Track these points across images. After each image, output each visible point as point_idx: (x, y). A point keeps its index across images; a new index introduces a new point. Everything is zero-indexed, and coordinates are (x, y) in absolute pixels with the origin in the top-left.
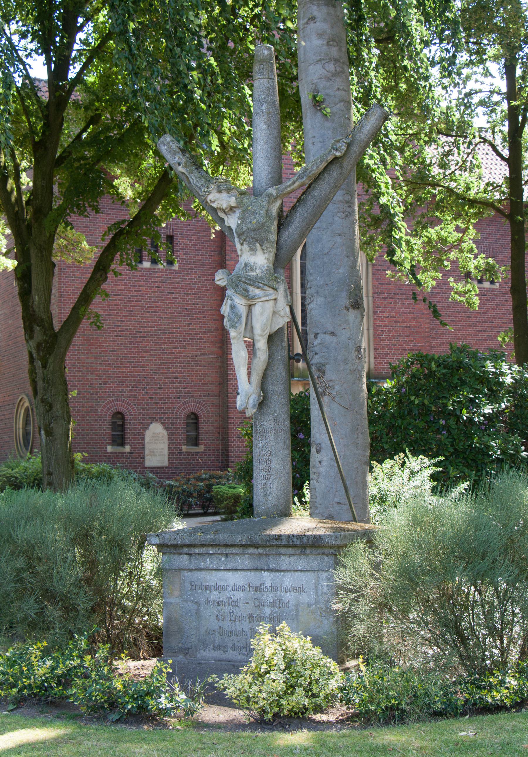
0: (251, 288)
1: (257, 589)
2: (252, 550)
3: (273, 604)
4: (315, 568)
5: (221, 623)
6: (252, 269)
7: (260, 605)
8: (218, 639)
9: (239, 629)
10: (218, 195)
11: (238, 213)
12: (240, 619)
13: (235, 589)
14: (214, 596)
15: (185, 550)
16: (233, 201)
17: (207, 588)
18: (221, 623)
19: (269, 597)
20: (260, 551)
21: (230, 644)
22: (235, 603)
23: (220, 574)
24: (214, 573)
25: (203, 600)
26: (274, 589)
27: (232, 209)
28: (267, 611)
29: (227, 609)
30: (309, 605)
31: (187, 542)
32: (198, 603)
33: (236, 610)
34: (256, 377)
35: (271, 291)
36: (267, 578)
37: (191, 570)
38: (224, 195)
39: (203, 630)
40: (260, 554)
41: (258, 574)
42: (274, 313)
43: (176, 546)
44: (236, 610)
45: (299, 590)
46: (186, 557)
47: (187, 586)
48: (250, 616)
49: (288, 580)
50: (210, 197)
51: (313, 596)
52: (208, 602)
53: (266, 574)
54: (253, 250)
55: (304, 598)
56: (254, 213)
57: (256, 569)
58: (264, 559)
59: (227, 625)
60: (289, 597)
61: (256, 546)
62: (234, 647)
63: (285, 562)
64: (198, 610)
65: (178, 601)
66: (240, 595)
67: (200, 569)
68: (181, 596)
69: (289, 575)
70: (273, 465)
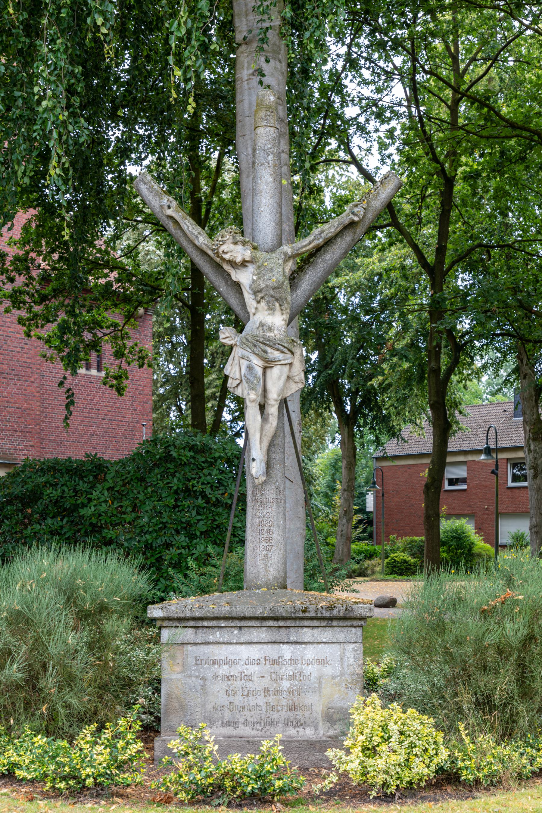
0: (269, 350)
1: (274, 662)
2: (271, 623)
3: (292, 677)
4: (341, 639)
5: (231, 699)
6: (270, 329)
7: (278, 678)
8: (227, 715)
9: (252, 703)
10: (232, 247)
11: (251, 268)
12: (254, 693)
13: (249, 662)
14: (224, 670)
15: (192, 623)
16: (248, 254)
17: (214, 663)
18: (231, 699)
19: (289, 670)
20: (281, 623)
21: (242, 720)
22: (249, 678)
23: (231, 648)
24: (224, 647)
25: (210, 675)
26: (293, 661)
27: (244, 264)
28: (286, 684)
29: (238, 684)
30: (334, 677)
31: (197, 614)
32: (204, 679)
33: (250, 685)
34: (266, 444)
35: (289, 355)
36: (287, 651)
37: (195, 644)
38: (240, 247)
39: (209, 707)
40: (280, 627)
41: (276, 646)
42: (289, 378)
43: (179, 619)
44: (250, 685)
45: (322, 662)
46: (191, 631)
47: (191, 661)
48: (266, 691)
49: (310, 653)
50: (224, 248)
51: (338, 668)
52: (216, 677)
53: (285, 646)
54: (271, 309)
55: (328, 670)
56: (271, 270)
57: (275, 642)
58: (283, 632)
59: (238, 700)
60: (312, 670)
61: (276, 619)
62: (246, 723)
63: (307, 634)
64: (203, 687)
65: (179, 676)
66: (254, 669)
67: (208, 643)
68: (183, 672)
69: (311, 647)
70: (274, 536)
